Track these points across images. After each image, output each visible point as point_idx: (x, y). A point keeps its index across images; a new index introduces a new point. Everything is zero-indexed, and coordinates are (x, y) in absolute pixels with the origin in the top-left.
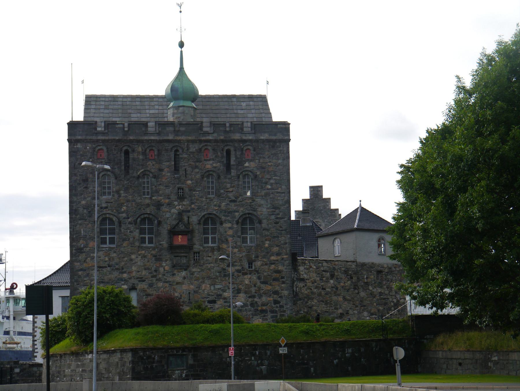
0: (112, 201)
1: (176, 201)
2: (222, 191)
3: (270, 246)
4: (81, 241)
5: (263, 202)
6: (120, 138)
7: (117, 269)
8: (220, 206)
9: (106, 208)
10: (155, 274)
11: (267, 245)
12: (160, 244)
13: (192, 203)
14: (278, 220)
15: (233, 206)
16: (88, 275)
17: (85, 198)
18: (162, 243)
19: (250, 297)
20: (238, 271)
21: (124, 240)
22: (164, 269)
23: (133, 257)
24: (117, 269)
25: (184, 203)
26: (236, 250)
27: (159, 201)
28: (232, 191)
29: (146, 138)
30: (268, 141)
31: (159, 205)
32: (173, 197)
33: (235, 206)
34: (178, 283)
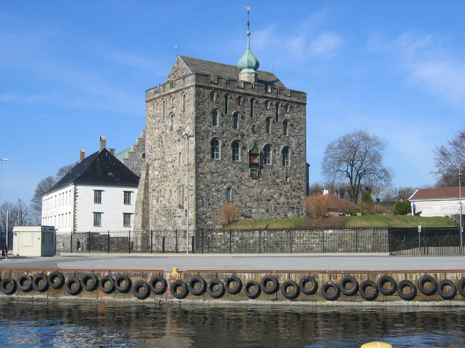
0: (219, 129)
1: (252, 134)
2: (274, 131)
3: (297, 168)
4: (202, 154)
5: (293, 140)
6: (224, 88)
7: (221, 175)
8: (273, 140)
9: (215, 133)
10: (241, 180)
11: (295, 167)
12: (243, 161)
13: (260, 136)
14: (300, 152)
15: (279, 141)
16: (205, 177)
17: (204, 125)
18: (244, 160)
19: (287, 199)
20: (282, 182)
21: (225, 156)
22: (245, 177)
23: (229, 168)
24: (221, 175)
25: (255, 135)
26: (280, 169)
27: (243, 133)
28: (279, 131)
29: (237, 90)
30: (297, 103)
31: (243, 135)
32: (250, 131)
33: (280, 141)
34: (252, 187)
